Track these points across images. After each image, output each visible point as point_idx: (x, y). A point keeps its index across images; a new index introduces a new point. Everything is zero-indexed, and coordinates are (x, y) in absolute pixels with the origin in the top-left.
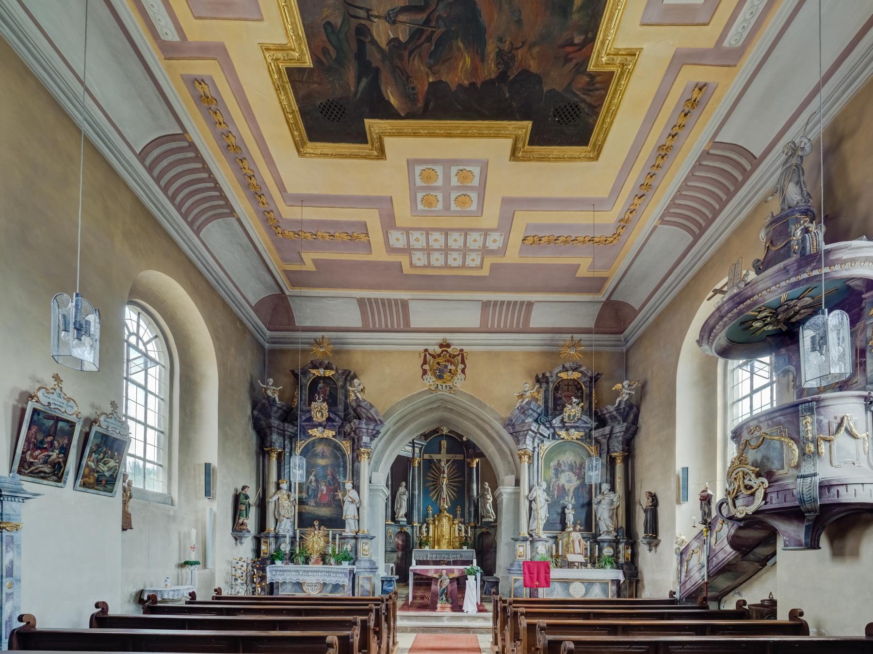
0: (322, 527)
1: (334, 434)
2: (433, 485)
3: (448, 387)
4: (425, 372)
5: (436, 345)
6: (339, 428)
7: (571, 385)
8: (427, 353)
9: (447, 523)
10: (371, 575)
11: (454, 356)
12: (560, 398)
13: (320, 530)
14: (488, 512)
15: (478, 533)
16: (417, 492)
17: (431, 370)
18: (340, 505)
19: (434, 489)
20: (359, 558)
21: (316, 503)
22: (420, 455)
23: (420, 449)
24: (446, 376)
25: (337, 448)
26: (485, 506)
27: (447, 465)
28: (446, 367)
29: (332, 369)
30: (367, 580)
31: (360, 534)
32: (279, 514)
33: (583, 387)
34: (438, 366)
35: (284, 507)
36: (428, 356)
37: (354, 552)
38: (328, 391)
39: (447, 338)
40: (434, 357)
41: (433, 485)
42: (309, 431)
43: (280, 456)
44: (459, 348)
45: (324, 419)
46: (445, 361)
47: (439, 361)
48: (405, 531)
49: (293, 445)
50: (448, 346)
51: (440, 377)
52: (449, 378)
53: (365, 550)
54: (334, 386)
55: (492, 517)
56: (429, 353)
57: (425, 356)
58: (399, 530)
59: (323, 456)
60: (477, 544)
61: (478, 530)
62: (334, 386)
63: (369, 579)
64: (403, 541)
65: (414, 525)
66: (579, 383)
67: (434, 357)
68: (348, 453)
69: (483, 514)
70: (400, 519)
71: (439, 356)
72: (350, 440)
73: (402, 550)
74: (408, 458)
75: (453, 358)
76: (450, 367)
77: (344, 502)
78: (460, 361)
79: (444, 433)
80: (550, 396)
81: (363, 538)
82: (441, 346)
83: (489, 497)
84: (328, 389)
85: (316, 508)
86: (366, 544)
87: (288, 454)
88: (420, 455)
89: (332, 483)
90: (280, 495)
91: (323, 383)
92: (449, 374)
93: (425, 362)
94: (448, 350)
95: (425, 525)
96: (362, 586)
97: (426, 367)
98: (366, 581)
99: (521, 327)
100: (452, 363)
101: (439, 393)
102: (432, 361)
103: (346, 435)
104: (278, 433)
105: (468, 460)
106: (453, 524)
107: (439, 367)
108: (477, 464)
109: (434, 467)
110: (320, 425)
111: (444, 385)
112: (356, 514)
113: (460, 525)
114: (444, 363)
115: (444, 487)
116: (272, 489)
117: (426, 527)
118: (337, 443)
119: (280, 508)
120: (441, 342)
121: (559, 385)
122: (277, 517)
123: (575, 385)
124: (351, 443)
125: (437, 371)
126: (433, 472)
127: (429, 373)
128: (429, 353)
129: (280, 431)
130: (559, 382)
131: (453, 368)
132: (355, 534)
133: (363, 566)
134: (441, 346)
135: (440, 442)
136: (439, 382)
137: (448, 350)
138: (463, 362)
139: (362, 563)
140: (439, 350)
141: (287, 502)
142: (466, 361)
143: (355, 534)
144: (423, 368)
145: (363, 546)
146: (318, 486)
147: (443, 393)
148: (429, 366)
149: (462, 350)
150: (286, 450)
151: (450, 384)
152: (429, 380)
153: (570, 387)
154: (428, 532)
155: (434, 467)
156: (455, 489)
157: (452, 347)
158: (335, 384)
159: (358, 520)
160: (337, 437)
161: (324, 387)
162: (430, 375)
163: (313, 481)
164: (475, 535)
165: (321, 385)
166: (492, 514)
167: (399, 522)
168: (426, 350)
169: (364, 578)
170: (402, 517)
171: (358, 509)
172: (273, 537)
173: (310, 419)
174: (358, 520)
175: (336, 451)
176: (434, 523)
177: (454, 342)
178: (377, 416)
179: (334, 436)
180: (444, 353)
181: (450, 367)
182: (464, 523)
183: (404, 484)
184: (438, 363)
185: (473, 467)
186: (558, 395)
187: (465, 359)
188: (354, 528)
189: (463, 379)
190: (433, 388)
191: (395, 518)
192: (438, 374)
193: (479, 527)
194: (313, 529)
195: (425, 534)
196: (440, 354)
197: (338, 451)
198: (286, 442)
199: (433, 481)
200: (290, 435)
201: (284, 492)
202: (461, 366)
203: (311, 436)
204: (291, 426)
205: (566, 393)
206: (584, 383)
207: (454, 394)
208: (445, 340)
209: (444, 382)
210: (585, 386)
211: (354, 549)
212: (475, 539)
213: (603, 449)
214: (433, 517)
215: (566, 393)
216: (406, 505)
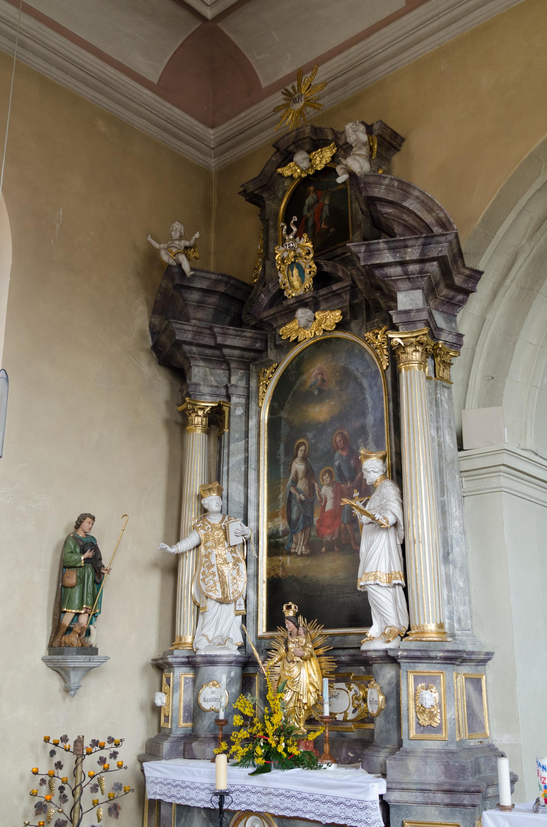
21: (309, 544)
29: (325, 143)
38: (326, 208)
45: (309, 282)
49: (253, 383)
84: (327, 202)
85: (308, 562)
87: (239, 411)
89: (346, 474)
104: (207, 359)
110: (302, 302)
129: (208, 352)
133: (415, 778)
139: (412, 764)
146: (311, 487)
159: (405, 590)
163: (300, 475)
172: (183, 664)
173: (280, 295)
174: (405, 590)
178: (430, 211)
179: (340, 326)
200: (242, 357)
204: (231, 330)
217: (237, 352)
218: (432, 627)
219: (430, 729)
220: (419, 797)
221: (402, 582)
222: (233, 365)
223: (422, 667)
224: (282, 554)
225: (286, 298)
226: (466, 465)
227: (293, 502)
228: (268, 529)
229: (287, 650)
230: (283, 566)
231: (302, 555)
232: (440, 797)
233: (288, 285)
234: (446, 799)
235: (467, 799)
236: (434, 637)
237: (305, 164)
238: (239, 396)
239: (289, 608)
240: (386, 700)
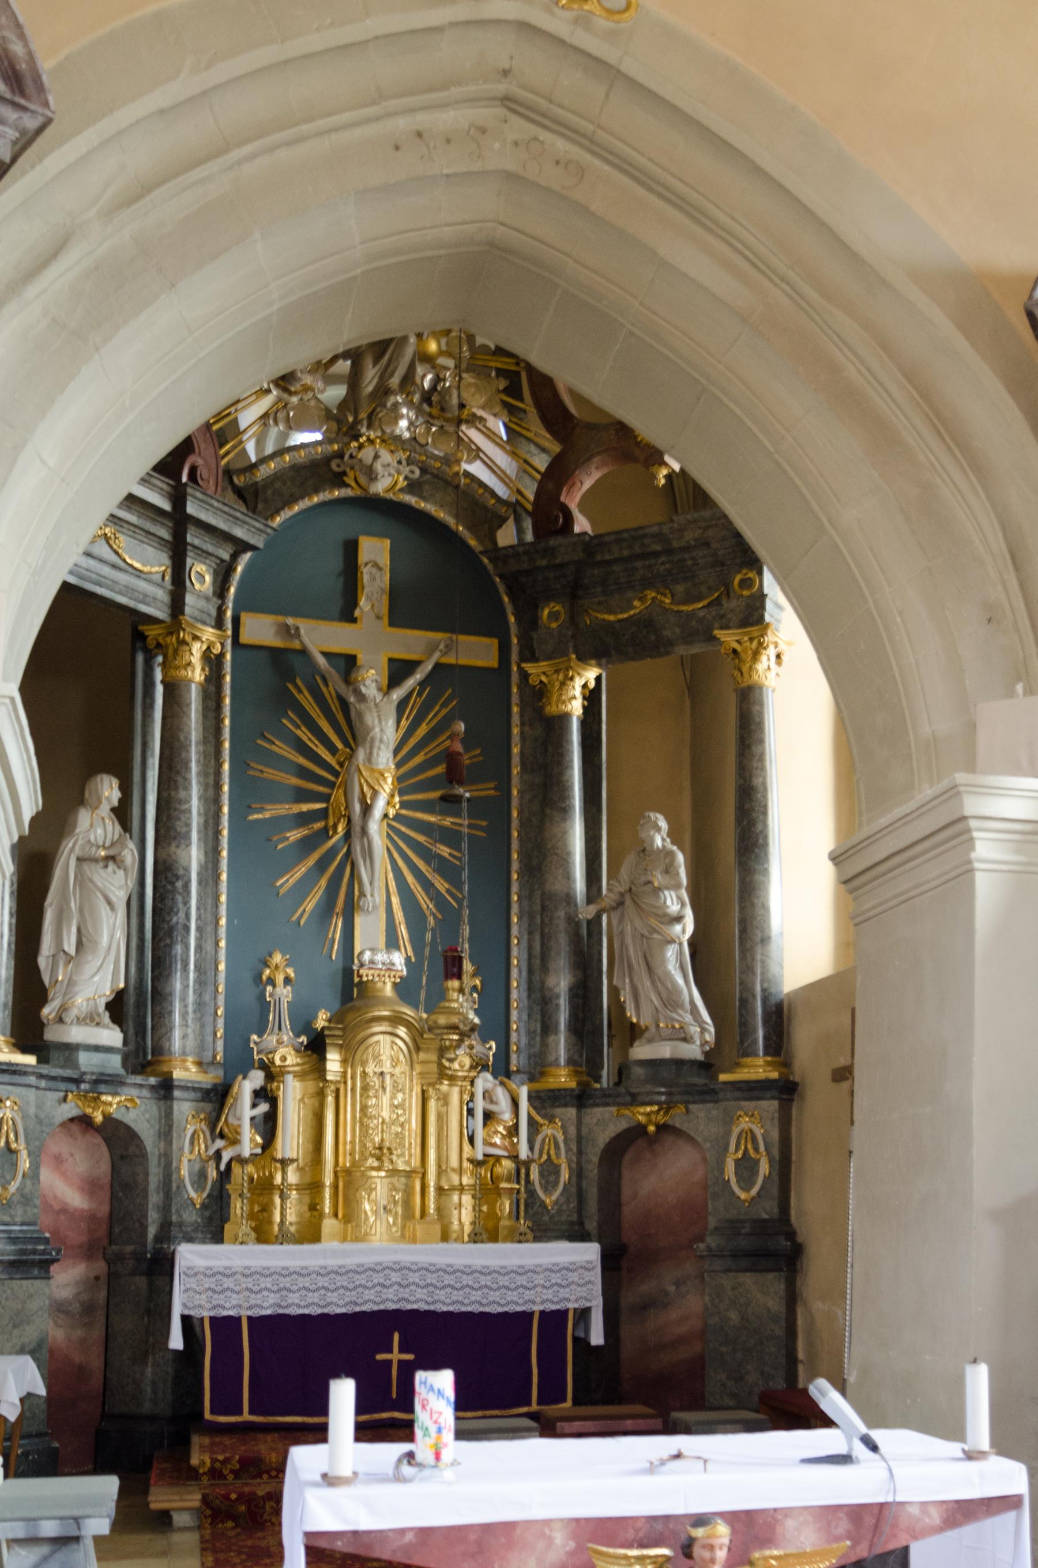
2: (303, 819)
9: (403, 1067)
14: (671, 1000)
15: (603, 1137)
16: (194, 856)
19: (307, 845)
22: (221, 612)
23: (223, 575)
26: (651, 966)
27: (397, 695)
41: (303, 819)
48: (108, 1118)
55: (695, 1030)
58: (70, 1109)
60: (592, 1205)
61: (596, 1114)
64: (90, 1187)
65: (177, 1074)
69: (630, 1013)
70: (76, 1034)
73: (89, 1251)
74: (137, 620)
79: (380, 487)
83: (674, 908)
88: (221, 612)
95: (256, 1079)
105: (530, 667)
106: (443, 1074)
108: (592, 697)
109: (306, 701)
113: (485, 1081)
115: (375, 826)
117: (261, 1094)
126: (304, 734)
135: (351, 548)
154: (268, 1125)
155: (306, 701)
156: (444, 851)
164: (580, 1153)
166: (694, 1011)
167: (70, 1049)
170: (90, 1019)
176: (319, 1069)
182: (502, 1070)
183: (109, 790)
185: (566, 717)
191: (40, 1026)
193: (607, 1098)
195: (249, 1141)
199: (302, 795)
212: (578, 1173)
214: (303, 1025)
216: (120, 935)
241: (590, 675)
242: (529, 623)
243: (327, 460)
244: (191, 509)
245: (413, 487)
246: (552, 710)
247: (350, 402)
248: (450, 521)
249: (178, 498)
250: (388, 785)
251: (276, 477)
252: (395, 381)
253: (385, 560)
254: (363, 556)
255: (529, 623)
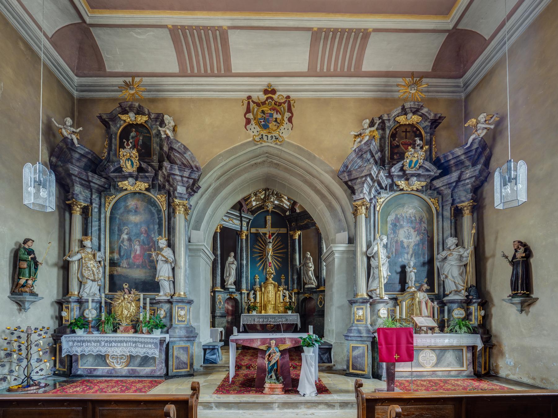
0: (133, 291)
1: (147, 187)
3: (274, 137)
4: (248, 122)
5: (260, 91)
6: (153, 180)
7: (408, 132)
8: (250, 101)
10: (188, 344)
11: (280, 104)
12: (398, 146)
13: (130, 293)
17: (255, 119)
18: (153, 267)
20: (174, 326)
21: (128, 264)
24: (272, 125)
25: (151, 202)
28: (271, 115)
30: (184, 351)
31: (175, 297)
32: (83, 276)
33: (423, 133)
34: (262, 115)
35: (88, 267)
36: (251, 103)
37: (168, 318)
39: (272, 83)
40: (258, 105)
42: (119, 183)
43: (85, 211)
44: (285, 94)
46: (270, 110)
47: (264, 109)
49: (103, 200)
50: (274, 92)
51: (265, 127)
52: (275, 128)
53: (180, 316)
54: (148, 135)
56: (253, 101)
57: (249, 103)
59: (136, 212)
62: (148, 135)
63: (186, 349)
66: (418, 129)
67: (258, 105)
68: (164, 207)
71: (264, 103)
72: (165, 193)
75: (279, 106)
76: (275, 116)
77: (157, 261)
78: (286, 109)
80: (387, 144)
81: (178, 302)
82: (266, 92)
86: (182, 309)
90: (83, 255)
91: (135, 131)
92: (275, 123)
93: (248, 111)
94: (274, 96)
96: (177, 357)
97: (250, 116)
98: (182, 351)
99: (352, 70)
100: (277, 112)
101: (264, 144)
102: (256, 110)
103: (161, 188)
107: (264, 116)
111: (269, 136)
112: (171, 275)
114: (269, 112)
116: (75, 247)
118: (151, 198)
119: (84, 268)
120: (265, 88)
121: (397, 132)
122: (80, 279)
123: (413, 132)
124: (167, 197)
125: (262, 121)
127: (253, 122)
128: (253, 101)
130: (397, 128)
131: (279, 116)
132: (169, 298)
133: (178, 334)
134: (266, 92)
136: (264, 132)
137: (274, 96)
138: (290, 110)
139: (177, 331)
140: (263, 97)
141: (92, 262)
142: (293, 109)
143: (169, 298)
144: (247, 116)
145: (180, 312)
147: (269, 144)
148: (253, 114)
149: (288, 97)
150: (94, 205)
151: (275, 134)
152: (253, 129)
153: (408, 133)
157: (278, 93)
158: (149, 132)
159: (174, 282)
160: (152, 190)
161: (136, 136)
162: (254, 125)
165: (133, 134)
168: (249, 98)
169: (180, 348)
171: (173, 269)
174: (174, 282)
175: (150, 207)
177: (280, 88)
179: (147, 190)
180: (269, 100)
181: (275, 116)
184: (263, 112)
186: (395, 143)
187: (292, 107)
188: (169, 291)
189: (290, 129)
190: (257, 139)
192: (263, 123)
194: (122, 294)
196: (265, 101)
197: (152, 206)
198: (94, 197)
200: (98, 188)
201: (89, 251)
202: (287, 115)
203: (122, 190)
205: (404, 140)
206: (424, 128)
207: (280, 145)
208: (269, 85)
209: (269, 132)
210: (426, 133)
211: (168, 315)
213: (447, 201)
215: (404, 140)
217: (96, 186)
218: (182, 293)
219: (182, 321)
220: (179, 339)
221: (173, 279)
222: (94, 191)
223: (180, 305)
224: (116, 267)
225: (123, 171)
226: (190, 247)
227: (122, 249)
228: (110, 257)
229: (124, 298)
230: (116, 270)
231: (125, 268)
232: (185, 339)
233: (125, 166)
234: (186, 339)
235: (192, 339)
236: (183, 296)
237: (133, 119)
238: (96, 204)
239: (126, 285)
240: (166, 314)
241: (299, 232)
242: (291, 226)
243: (262, 205)
244: (242, 215)
245: (274, 208)
246: (294, 238)
247: (265, 197)
248: (279, 212)
249: (240, 214)
250: (271, 251)
251: (255, 209)
252: (271, 193)
253: (270, 219)
254: (267, 219)
255: (291, 226)
